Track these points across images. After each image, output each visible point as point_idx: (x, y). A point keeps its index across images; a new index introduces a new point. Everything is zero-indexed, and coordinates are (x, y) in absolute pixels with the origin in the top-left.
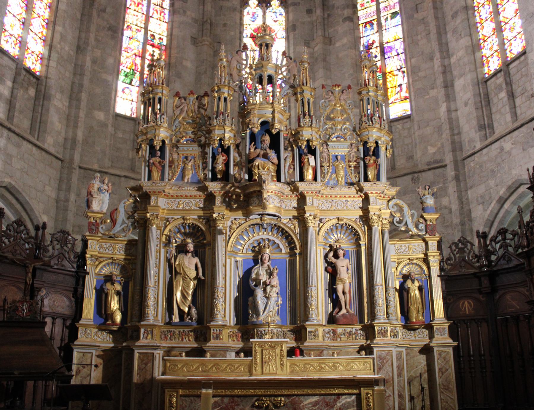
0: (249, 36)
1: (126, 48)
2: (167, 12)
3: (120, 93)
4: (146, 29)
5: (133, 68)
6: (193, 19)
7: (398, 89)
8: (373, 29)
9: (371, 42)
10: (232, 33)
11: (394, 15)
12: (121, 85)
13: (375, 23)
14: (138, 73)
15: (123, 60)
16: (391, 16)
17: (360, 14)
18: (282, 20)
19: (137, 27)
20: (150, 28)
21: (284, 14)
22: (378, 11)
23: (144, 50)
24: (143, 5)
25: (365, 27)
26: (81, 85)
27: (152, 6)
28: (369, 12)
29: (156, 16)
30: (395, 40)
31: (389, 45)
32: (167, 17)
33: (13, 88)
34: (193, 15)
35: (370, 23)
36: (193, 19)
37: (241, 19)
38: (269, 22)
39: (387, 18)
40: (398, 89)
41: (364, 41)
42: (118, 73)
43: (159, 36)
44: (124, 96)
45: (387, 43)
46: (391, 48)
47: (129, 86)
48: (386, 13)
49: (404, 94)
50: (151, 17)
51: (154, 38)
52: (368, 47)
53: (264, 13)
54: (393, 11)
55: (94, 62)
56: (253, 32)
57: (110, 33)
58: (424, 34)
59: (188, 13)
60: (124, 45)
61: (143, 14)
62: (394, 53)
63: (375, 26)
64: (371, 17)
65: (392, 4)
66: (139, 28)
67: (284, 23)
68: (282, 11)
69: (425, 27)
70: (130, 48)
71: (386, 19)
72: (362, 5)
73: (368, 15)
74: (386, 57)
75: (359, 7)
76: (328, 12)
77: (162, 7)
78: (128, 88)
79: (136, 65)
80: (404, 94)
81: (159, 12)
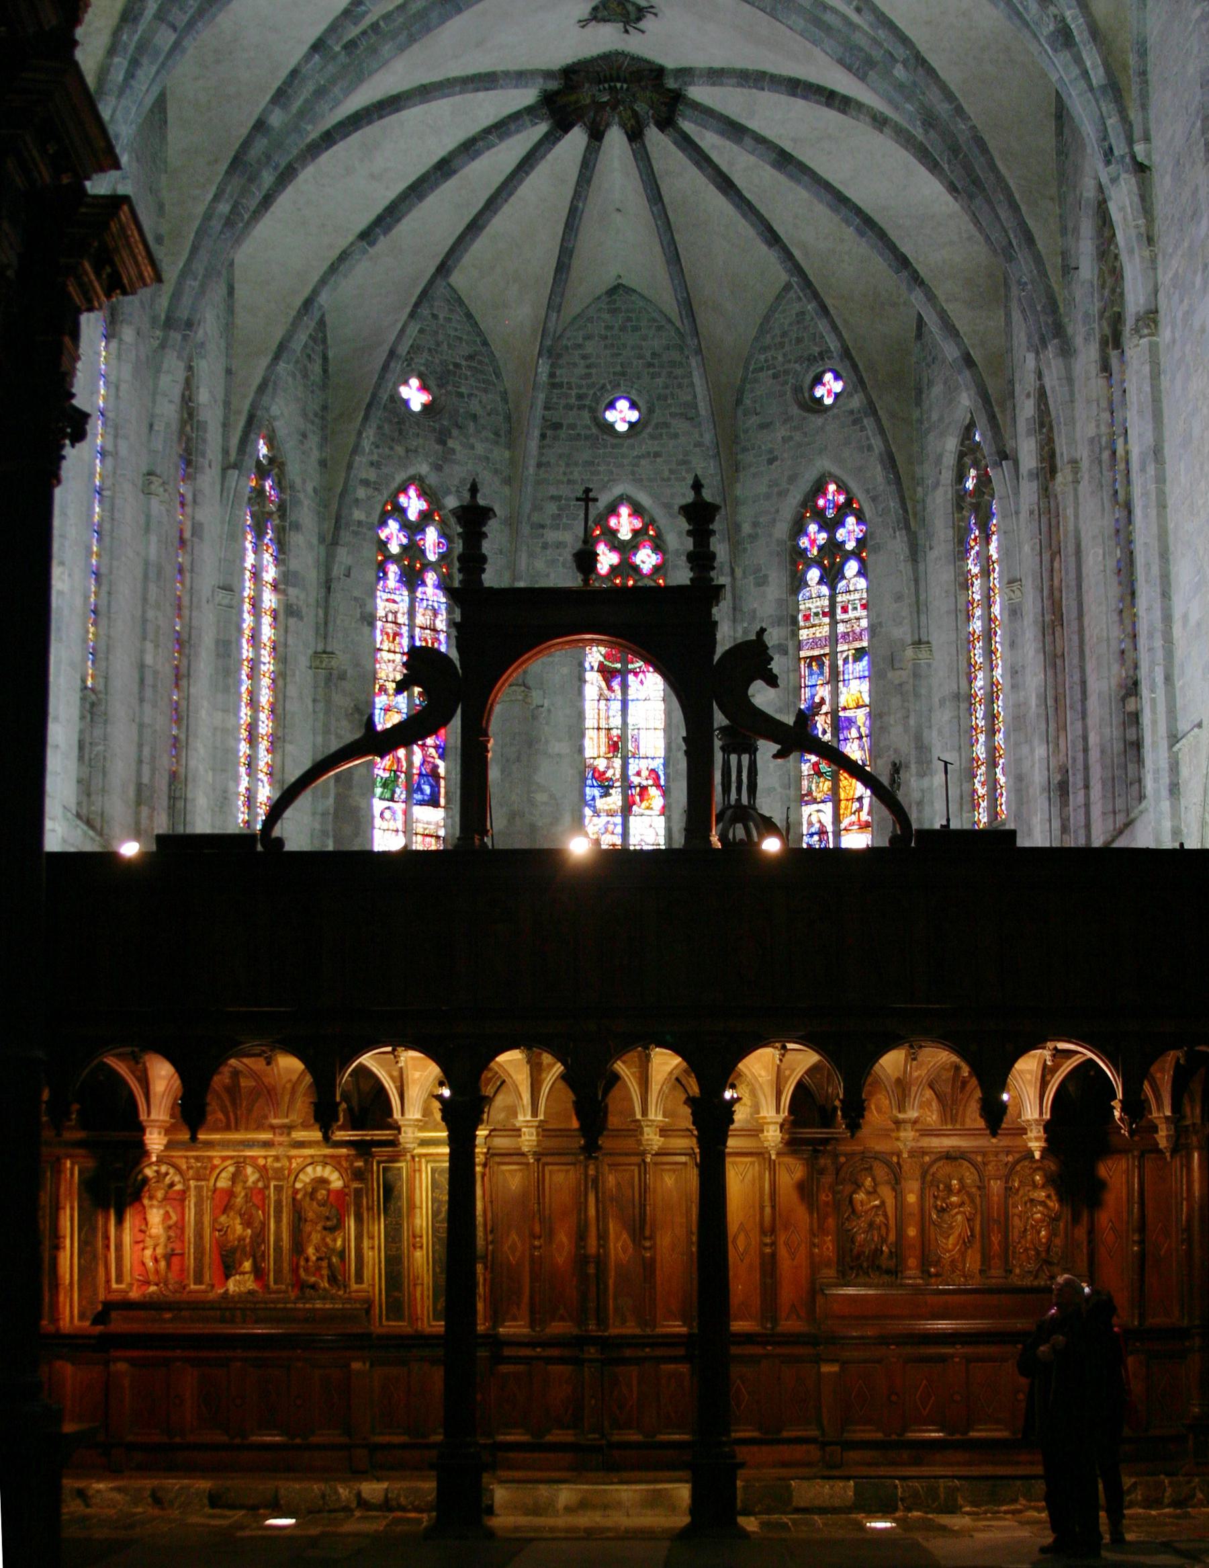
0: (596, 666)
3: (378, 822)
5: (395, 767)
7: (856, 805)
8: (822, 673)
9: (817, 700)
11: (860, 654)
12: (378, 805)
13: (827, 663)
14: (403, 776)
16: (854, 655)
17: (804, 634)
22: (833, 639)
24: (401, 635)
25: (810, 666)
27: (417, 630)
28: (818, 635)
30: (858, 707)
31: (848, 714)
35: (818, 659)
39: (847, 657)
40: (856, 805)
41: (806, 693)
44: (385, 825)
45: (844, 709)
46: (850, 721)
47: (391, 804)
48: (845, 647)
49: (864, 816)
52: (815, 708)
54: (858, 645)
56: (602, 659)
58: (899, 715)
62: (854, 733)
63: (826, 670)
64: (822, 648)
65: (858, 630)
69: (903, 701)
71: (846, 661)
72: (807, 618)
73: (815, 643)
74: (841, 737)
75: (802, 624)
76: (745, 625)
77: (434, 630)
78: (388, 808)
80: (864, 816)
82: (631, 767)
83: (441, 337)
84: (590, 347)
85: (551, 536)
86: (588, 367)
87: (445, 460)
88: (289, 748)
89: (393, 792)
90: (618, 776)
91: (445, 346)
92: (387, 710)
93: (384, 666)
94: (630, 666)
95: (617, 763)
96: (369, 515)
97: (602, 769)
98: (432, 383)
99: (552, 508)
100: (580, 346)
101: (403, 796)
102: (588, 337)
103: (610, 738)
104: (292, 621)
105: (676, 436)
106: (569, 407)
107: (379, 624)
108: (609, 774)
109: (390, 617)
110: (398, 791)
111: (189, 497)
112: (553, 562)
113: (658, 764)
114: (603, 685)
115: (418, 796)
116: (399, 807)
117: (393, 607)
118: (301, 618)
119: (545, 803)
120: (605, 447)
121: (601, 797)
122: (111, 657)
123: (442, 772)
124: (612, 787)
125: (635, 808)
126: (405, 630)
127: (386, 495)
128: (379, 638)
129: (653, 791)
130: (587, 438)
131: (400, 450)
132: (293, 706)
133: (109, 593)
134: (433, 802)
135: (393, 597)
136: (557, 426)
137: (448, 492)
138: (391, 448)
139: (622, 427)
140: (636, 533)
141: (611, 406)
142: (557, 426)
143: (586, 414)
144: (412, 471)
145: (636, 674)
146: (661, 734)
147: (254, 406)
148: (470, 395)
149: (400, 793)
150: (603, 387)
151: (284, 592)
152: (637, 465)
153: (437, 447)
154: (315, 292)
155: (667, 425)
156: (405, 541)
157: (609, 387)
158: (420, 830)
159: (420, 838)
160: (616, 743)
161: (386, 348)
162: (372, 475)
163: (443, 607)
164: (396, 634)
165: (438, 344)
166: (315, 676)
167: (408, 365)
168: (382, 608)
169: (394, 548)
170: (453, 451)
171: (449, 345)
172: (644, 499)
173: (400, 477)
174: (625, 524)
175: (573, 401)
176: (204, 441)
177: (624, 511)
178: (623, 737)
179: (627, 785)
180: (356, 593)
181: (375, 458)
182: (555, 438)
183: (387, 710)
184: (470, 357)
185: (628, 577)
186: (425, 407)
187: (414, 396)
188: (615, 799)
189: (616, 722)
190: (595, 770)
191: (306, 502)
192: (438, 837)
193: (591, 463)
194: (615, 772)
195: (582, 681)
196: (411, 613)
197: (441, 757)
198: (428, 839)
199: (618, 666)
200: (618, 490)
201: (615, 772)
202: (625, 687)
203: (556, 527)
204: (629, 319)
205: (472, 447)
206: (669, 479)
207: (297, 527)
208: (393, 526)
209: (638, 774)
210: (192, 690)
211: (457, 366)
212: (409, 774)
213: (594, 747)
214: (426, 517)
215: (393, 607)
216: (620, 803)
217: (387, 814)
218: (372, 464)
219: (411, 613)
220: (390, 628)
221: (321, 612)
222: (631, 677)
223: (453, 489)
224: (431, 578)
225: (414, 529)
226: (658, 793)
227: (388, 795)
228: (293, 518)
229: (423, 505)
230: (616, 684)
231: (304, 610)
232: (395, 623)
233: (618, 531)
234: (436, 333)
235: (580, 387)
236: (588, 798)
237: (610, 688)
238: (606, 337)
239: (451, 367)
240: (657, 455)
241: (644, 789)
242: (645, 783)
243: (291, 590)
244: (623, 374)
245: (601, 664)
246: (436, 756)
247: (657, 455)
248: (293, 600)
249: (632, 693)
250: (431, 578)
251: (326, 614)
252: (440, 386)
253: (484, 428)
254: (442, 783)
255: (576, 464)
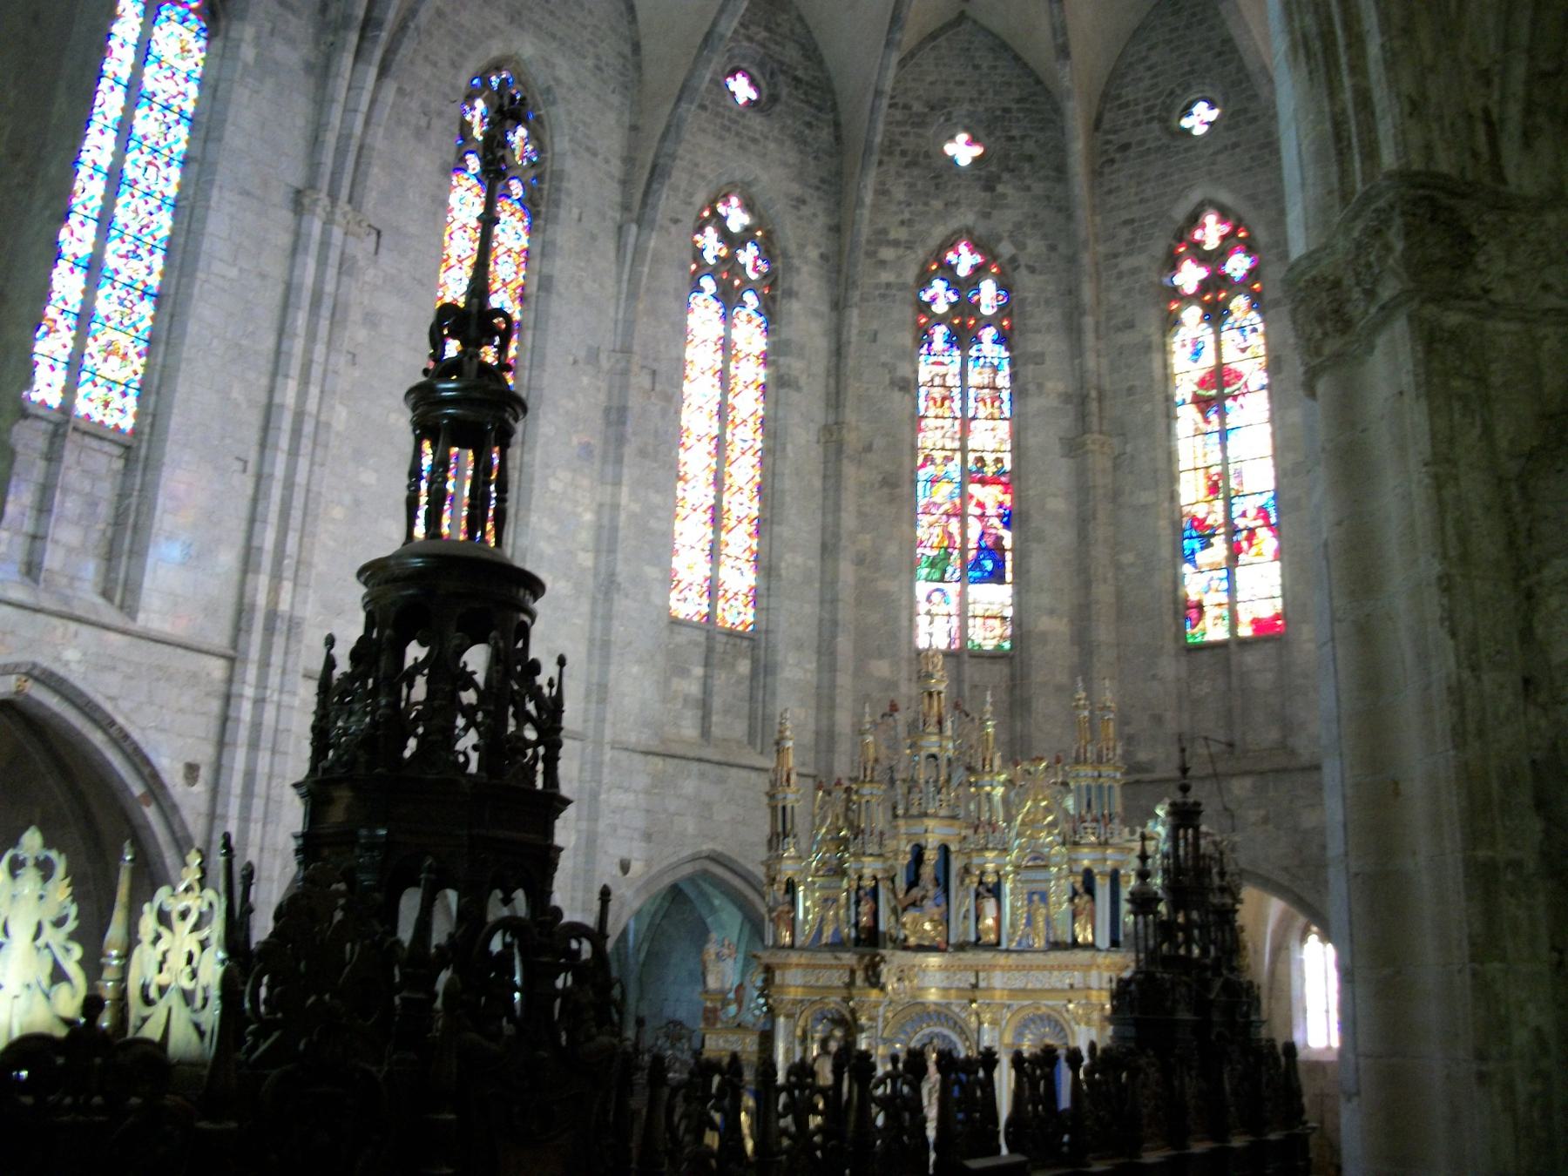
0: (1189, 400)
1: (927, 506)
2: (1005, 395)
4: (964, 450)
5: (946, 543)
6: (1060, 395)
10: (1147, 408)
12: (922, 589)
15: (921, 533)
18: (1257, 342)
19: (944, 453)
20: (971, 444)
21: (1261, 327)
23: (965, 497)
26: (835, 623)
27: (972, 393)
29: (983, 412)
32: (1006, 407)
33: (706, 677)
34: (1061, 387)
36: (1060, 395)
37: (1166, 365)
38: (1230, 356)
42: (914, 564)
43: (994, 456)
47: (940, 585)
50: (974, 418)
51: (984, 465)
53: (1218, 333)
55: (860, 561)
57: (886, 490)
59: (1050, 385)
60: (922, 502)
61: (955, 418)
66: (949, 453)
67: (1262, 351)
68: (1254, 317)
70: (935, 504)
77: (994, 388)
79: (950, 536)
81: (989, 402)
82: (1234, 508)
83: (984, 86)
84: (1154, 57)
85: (1126, 263)
86: (1155, 76)
87: (994, 206)
88: (776, 529)
89: (944, 571)
90: (1221, 520)
91: (990, 94)
92: (934, 481)
93: (929, 434)
94: (1227, 390)
95: (1219, 505)
96: (899, 275)
97: (1201, 515)
98: (981, 134)
99: (1125, 233)
100: (1144, 59)
101: (958, 574)
102: (1151, 48)
103: (1209, 478)
104: (782, 392)
105: (1255, 119)
106: (1137, 124)
107: (923, 391)
108: (1209, 522)
109: (937, 381)
110: (950, 570)
111: (536, 250)
112: (1128, 293)
113: (1266, 499)
114: (1199, 417)
115: (978, 574)
116: (953, 589)
117: (941, 370)
118: (799, 389)
119: (1132, 565)
120: (1177, 153)
121: (1202, 548)
122: (163, 390)
123: (1008, 543)
124: (1213, 535)
125: (1241, 557)
126: (956, 393)
127: (921, 253)
128: (922, 404)
129: (1264, 535)
130: (1159, 149)
131: (937, 204)
132: (788, 483)
133: (172, 316)
134: (997, 576)
135: (941, 359)
136: (1125, 147)
137: (999, 240)
138: (926, 204)
139: (1200, 130)
140: (1224, 238)
141: (1187, 111)
142: (1125, 147)
143: (1155, 125)
144: (954, 224)
145: (1235, 398)
146: (1270, 462)
147: (657, 156)
148: (1023, 138)
149: (953, 571)
150: (1172, 93)
151: (774, 363)
152: (1214, 163)
153: (983, 194)
154: (715, 24)
155: (1245, 111)
156: (954, 298)
157: (1179, 91)
158: (979, 612)
159: (979, 621)
160: (1216, 483)
161: (872, 88)
162: (901, 234)
163: (1005, 362)
164: (944, 399)
165: (981, 93)
166: (826, 450)
167: (947, 120)
168: (925, 372)
169: (940, 308)
170: (1004, 196)
171: (996, 93)
172: (1225, 197)
173: (939, 232)
174: (1211, 232)
175: (1140, 117)
176: (558, 190)
177: (1211, 219)
178: (1224, 475)
179: (1232, 530)
180: (883, 358)
181: (907, 216)
182: (1125, 160)
183: (934, 481)
184: (1019, 101)
185: (1218, 290)
186: (977, 161)
187: (962, 150)
188: (1219, 549)
189: (1216, 457)
190: (1194, 518)
191: (805, 269)
192: (1003, 618)
193: (1164, 175)
194: (1216, 517)
195: (1170, 417)
196: (963, 374)
197: (1007, 525)
198: (990, 622)
199: (1213, 392)
200: (1196, 196)
201: (1216, 517)
202: (1222, 413)
203: (1129, 253)
204: (1194, 15)
205: (1028, 189)
206: (1249, 169)
207: (790, 294)
208: (939, 286)
209: (1244, 515)
210: (527, 458)
211: (1006, 110)
212: (964, 551)
213: (1191, 493)
214: (979, 271)
215: (941, 370)
216: (1225, 553)
217: (936, 597)
218: (902, 223)
219: (963, 374)
220: (937, 393)
221: (832, 382)
222: (1229, 403)
223: (1006, 235)
224: (989, 334)
225: (964, 287)
226: (1270, 534)
227: (937, 575)
228: (786, 286)
229: (978, 259)
230: (1214, 418)
231: (803, 380)
232: (943, 386)
233: (1203, 242)
234: (979, 83)
235: (1147, 100)
236: (1187, 552)
237: (1207, 421)
238: (1171, 41)
239: (998, 113)
240: (1235, 145)
241: (1252, 532)
242: (1252, 525)
243: (782, 360)
244: (1192, 72)
245: (1195, 394)
246: (1000, 526)
247: (1235, 145)
248: (783, 371)
249: (1231, 421)
250: (989, 334)
251: (838, 383)
252: (988, 135)
253: (1042, 167)
254: (1009, 556)
255: (1148, 181)
